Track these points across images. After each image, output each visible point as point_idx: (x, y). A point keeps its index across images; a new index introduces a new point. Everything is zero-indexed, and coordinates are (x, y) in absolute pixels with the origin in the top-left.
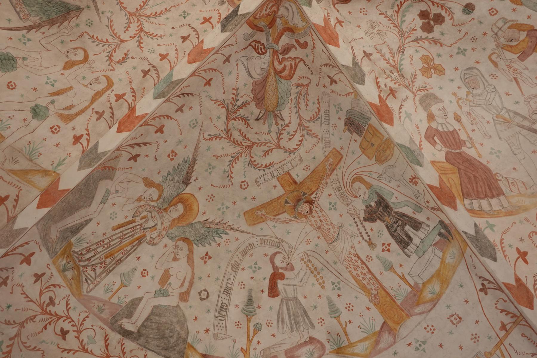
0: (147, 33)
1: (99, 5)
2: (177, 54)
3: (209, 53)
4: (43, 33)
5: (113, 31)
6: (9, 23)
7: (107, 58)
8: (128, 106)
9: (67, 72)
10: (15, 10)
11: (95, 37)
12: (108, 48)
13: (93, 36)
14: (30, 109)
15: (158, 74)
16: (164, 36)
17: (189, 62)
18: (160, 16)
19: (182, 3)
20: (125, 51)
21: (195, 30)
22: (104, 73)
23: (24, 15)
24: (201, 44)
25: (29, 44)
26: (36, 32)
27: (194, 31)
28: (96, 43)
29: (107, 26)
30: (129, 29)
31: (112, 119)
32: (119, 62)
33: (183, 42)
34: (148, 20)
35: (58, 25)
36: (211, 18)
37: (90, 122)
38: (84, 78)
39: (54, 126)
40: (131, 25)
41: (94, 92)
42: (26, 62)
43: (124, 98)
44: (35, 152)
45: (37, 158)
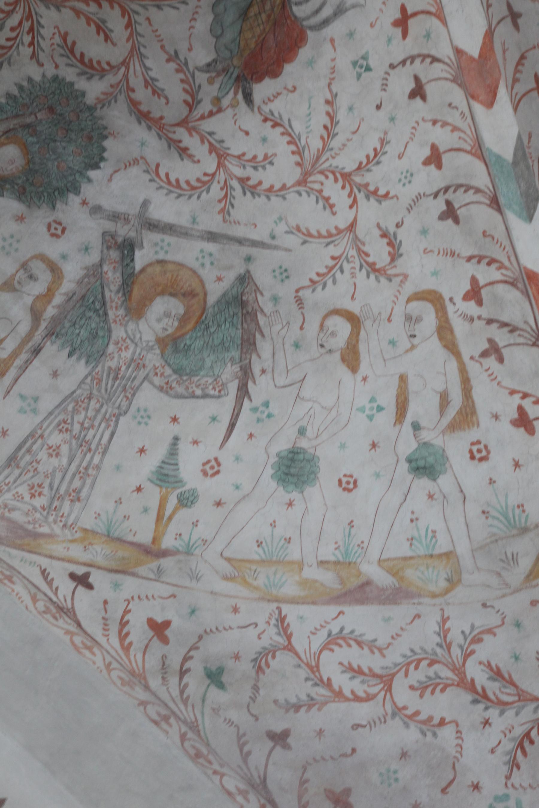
0: (359, 168)
1: (255, 236)
2: (445, 124)
3: (492, 49)
4: (263, 371)
5: (320, 236)
6: (218, 421)
7: (372, 277)
8: (507, 287)
9: (364, 369)
10: (198, 397)
11: (316, 278)
12: (352, 265)
13: (311, 280)
14: (411, 477)
15: (468, 188)
16: (386, 133)
17: (490, 104)
18: (337, 123)
19: (333, 60)
20: (378, 233)
21: (412, 59)
22: (403, 298)
23: (214, 388)
24: (464, 57)
25: (274, 408)
26: (254, 382)
27: (412, 63)
28: (330, 283)
29: (304, 242)
30: (331, 201)
31: (518, 333)
32: (394, 257)
33: (424, 98)
34: (333, 153)
35: (258, 336)
36: (403, 9)
37: (499, 379)
38: (392, 343)
39: (471, 452)
40: (326, 194)
41: (435, 339)
42: (309, 433)
43: (482, 283)
44: (511, 515)
45: (527, 516)
